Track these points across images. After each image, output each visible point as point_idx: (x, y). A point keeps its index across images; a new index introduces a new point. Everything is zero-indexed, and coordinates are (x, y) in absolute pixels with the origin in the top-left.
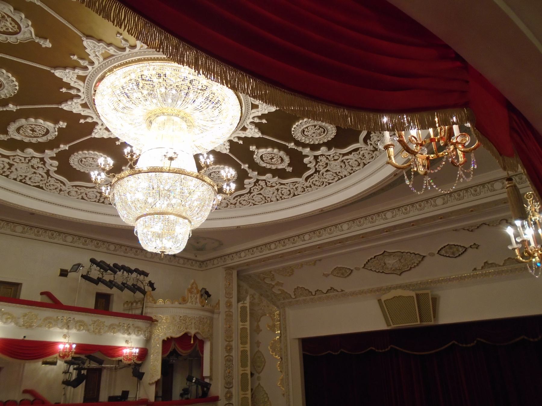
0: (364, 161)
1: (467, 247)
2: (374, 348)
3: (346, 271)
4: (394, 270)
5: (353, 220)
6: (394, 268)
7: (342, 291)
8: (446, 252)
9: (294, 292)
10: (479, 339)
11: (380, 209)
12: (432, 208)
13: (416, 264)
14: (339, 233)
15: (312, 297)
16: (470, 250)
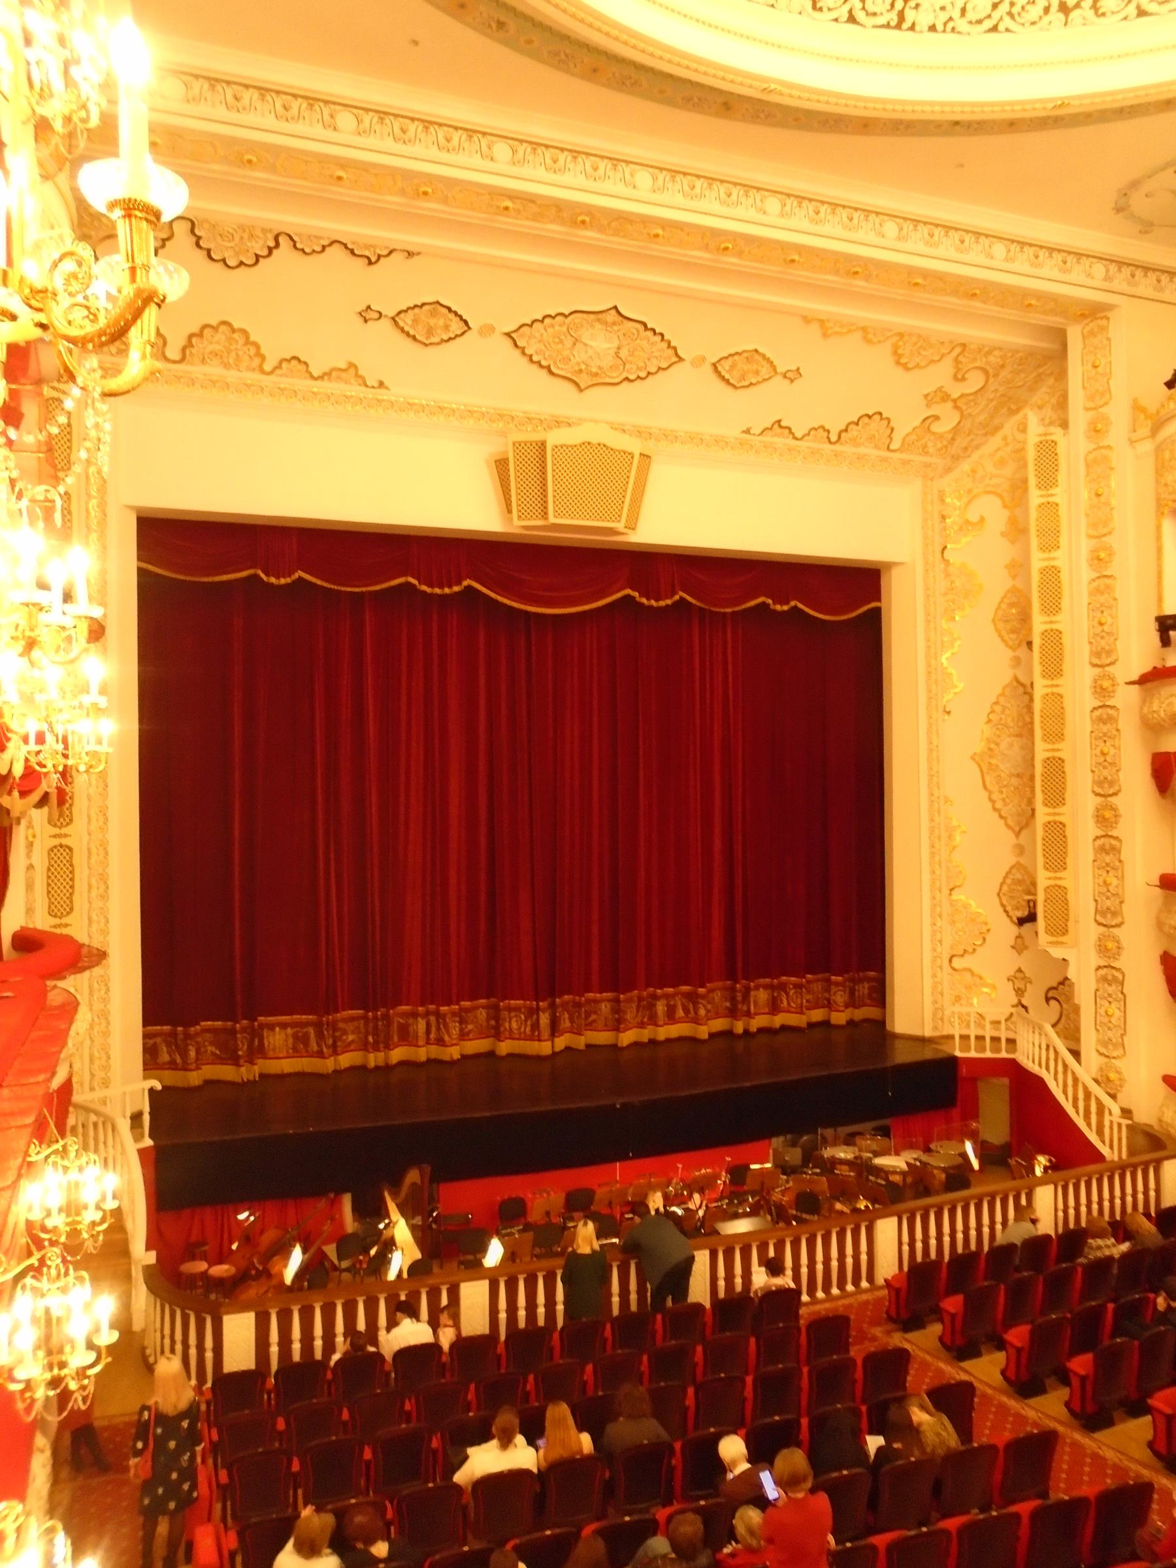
0: (1007, 19)
1: (781, 369)
2: (415, 582)
3: (447, 327)
4: (581, 371)
5: (674, 173)
6: (583, 367)
7: (381, 384)
8: (733, 367)
9: (191, 336)
10: (681, 593)
11: (762, 178)
12: (872, 238)
13: (643, 374)
14: (620, 189)
15: (256, 376)
16: (779, 378)
